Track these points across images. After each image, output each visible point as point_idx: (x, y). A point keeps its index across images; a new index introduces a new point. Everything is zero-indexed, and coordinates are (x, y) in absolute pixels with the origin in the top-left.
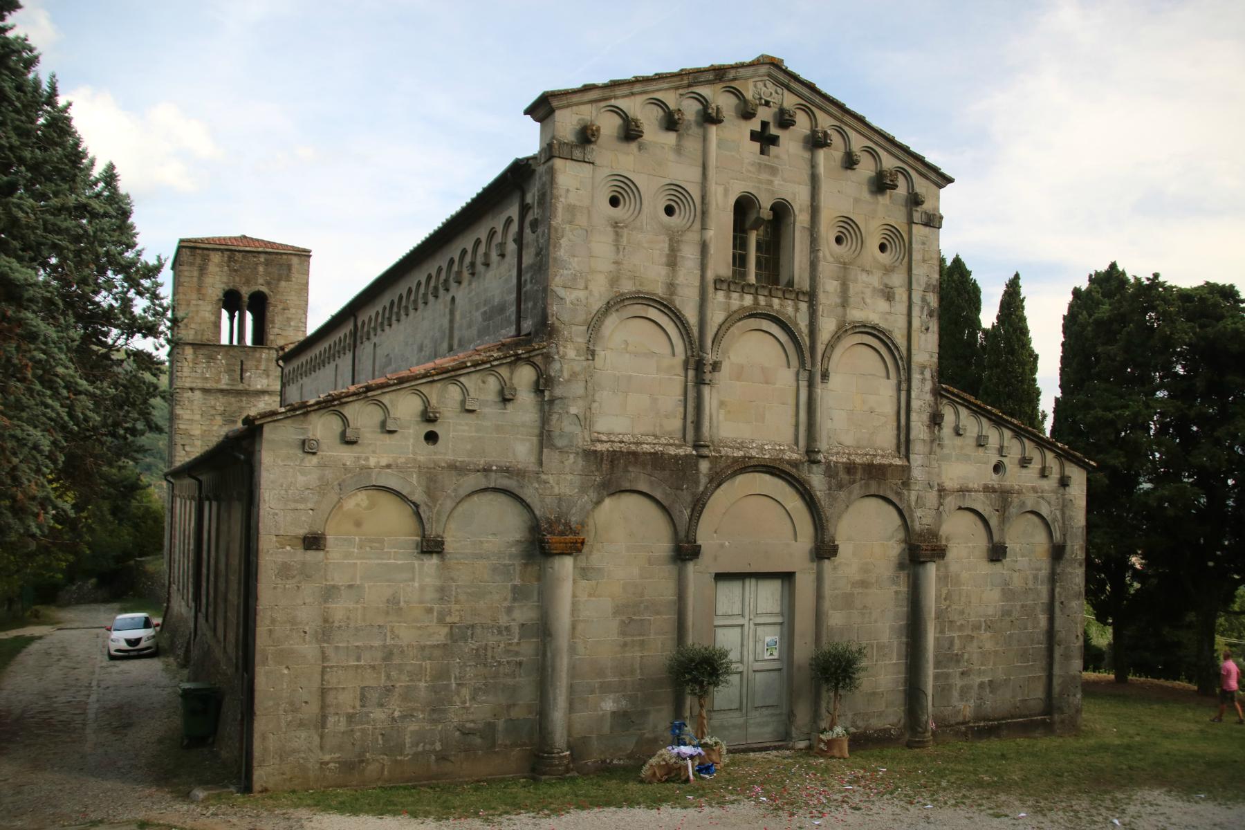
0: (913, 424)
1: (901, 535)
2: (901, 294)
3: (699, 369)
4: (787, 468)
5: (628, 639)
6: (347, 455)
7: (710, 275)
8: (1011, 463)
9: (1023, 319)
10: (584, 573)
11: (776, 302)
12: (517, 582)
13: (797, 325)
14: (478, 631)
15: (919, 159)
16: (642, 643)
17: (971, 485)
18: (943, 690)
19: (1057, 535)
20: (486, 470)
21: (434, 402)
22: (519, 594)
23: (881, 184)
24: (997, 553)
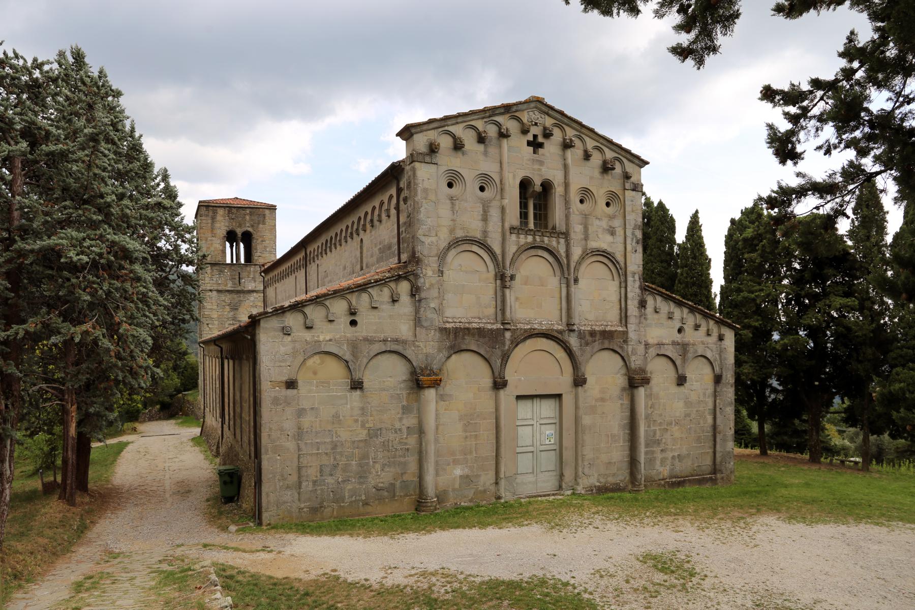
0: (629, 307)
1: (624, 371)
2: (620, 231)
3: (503, 279)
4: (556, 334)
5: (468, 434)
6: (308, 336)
7: (507, 226)
8: (688, 328)
9: (701, 238)
10: (441, 397)
11: (546, 239)
12: (405, 403)
13: (558, 252)
14: (384, 432)
15: (628, 152)
16: (476, 435)
17: (664, 341)
18: (651, 461)
19: (717, 369)
20: (385, 341)
21: (354, 303)
22: (406, 410)
23: (606, 168)
24: (681, 380)
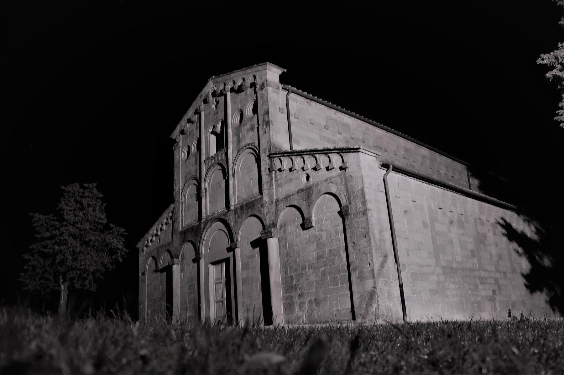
19: (344, 201)
